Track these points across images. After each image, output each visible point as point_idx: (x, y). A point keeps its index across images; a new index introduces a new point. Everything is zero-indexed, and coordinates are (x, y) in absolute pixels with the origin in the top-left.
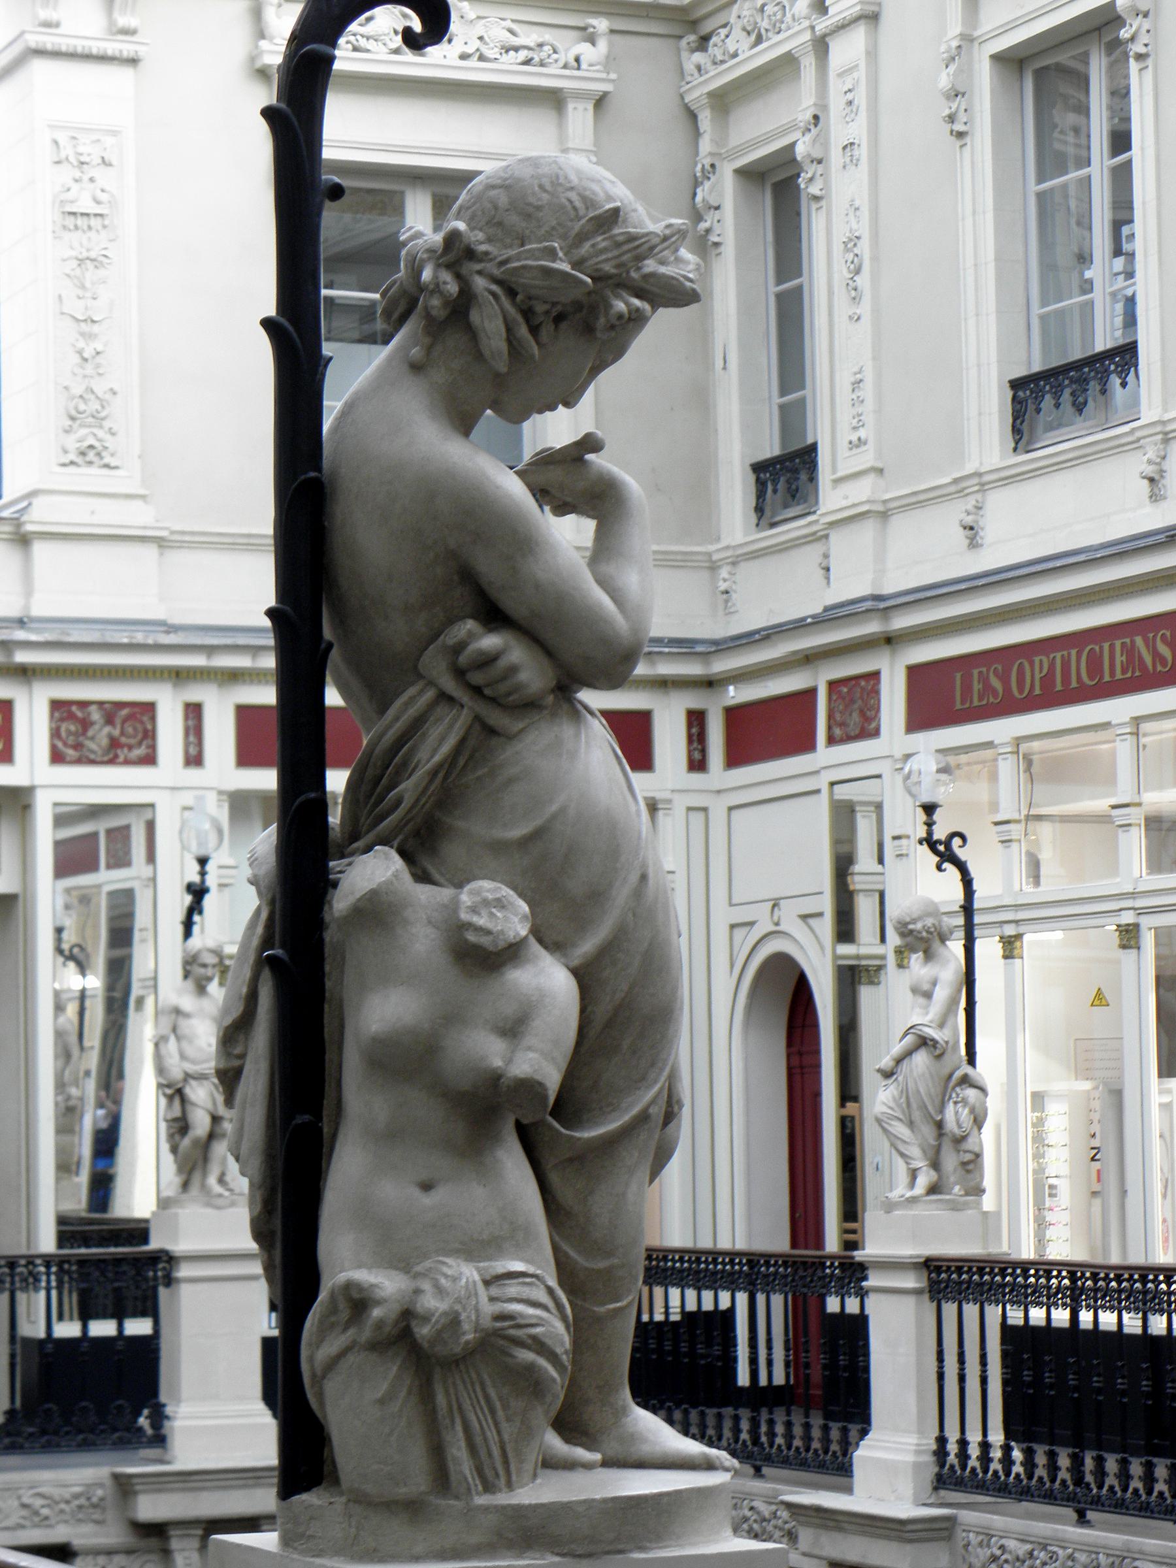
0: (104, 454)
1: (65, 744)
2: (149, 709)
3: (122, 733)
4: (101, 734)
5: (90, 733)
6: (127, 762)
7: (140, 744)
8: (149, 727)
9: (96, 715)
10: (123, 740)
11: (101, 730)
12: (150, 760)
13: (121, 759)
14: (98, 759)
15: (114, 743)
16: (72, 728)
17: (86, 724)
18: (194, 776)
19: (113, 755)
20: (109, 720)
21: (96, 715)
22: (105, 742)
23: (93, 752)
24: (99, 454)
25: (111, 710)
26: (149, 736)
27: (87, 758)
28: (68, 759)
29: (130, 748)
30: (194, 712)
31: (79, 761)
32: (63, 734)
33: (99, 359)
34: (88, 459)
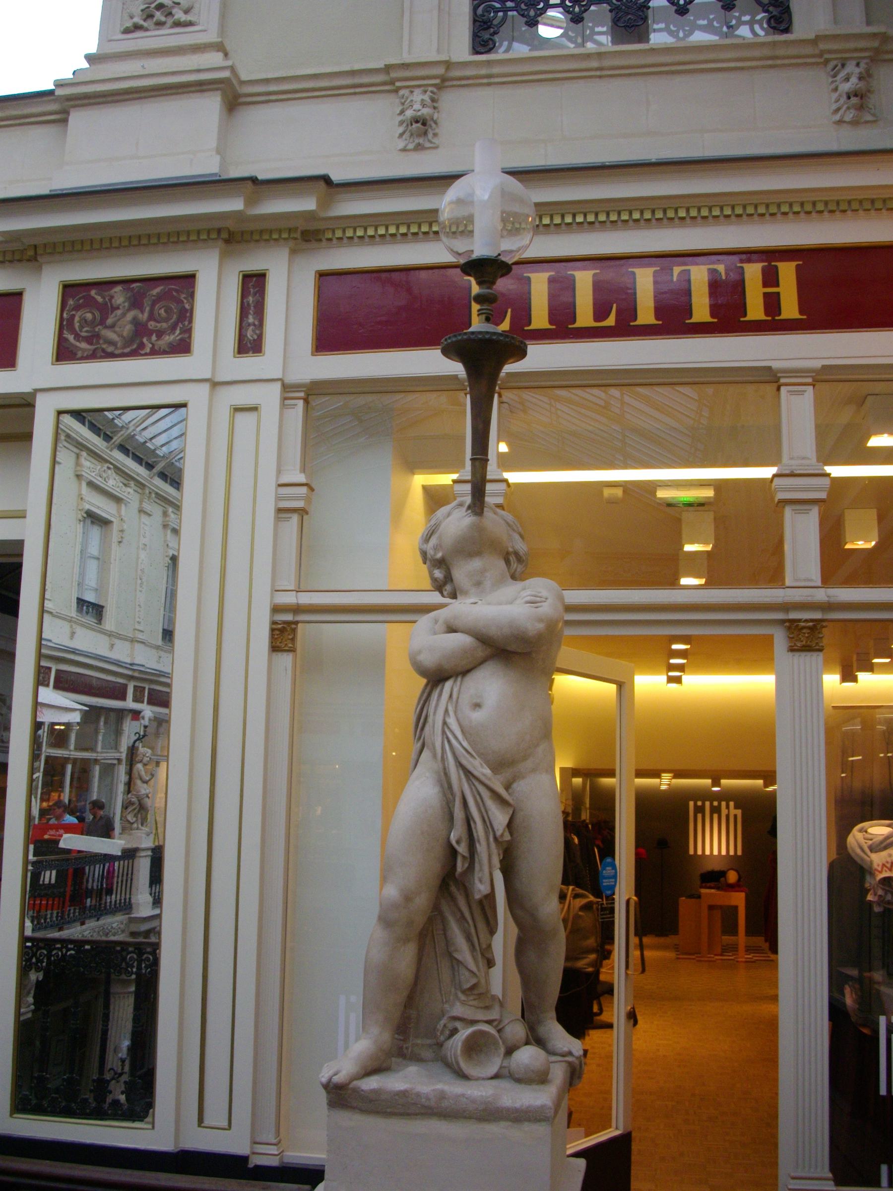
1: (78, 337)
3: (151, 317)
5: (109, 321)
6: (155, 352)
7: (173, 328)
8: (187, 306)
9: (119, 297)
10: (152, 325)
12: (183, 347)
13: (148, 350)
14: (117, 352)
15: (140, 330)
16: (89, 316)
17: (106, 309)
20: (136, 303)
22: (127, 329)
26: (186, 316)
27: (103, 350)
28: (79, 354)
29: (160, 334)
31: (93, 356)
32: (77, 325)
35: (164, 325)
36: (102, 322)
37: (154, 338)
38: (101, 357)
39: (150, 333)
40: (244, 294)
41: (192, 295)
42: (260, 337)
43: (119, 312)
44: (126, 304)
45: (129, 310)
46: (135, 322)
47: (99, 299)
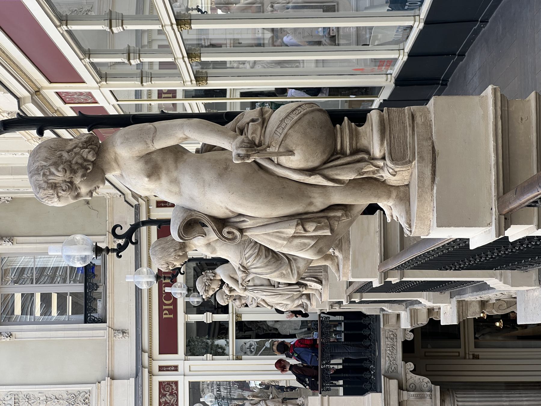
0: (86, 396)
2: (161, 383)
3: (168, 391)
4: (168, 398)
5: (169, 402)
6: (177, 390)
7: (171, 386)
9: (163, 400)
11: (167, 398)
12: (176, 383)
15: (171, 394)
18: (180, 368)
19: (175, 394)
20: (165, 395)
21: (163, 400)
22: (171, 397)
23: (174, 401)
24: (86, 398)
25: (162, 395)
26: (169, 383)
29: (173, 389)
30: (161, 368)
33: (57, 397)
34: (88, 401)
35: (171, 388)
36: (169, 403)
37: (173, 390)
38: (177, 403)
39: (172, 391)
40: (164, 371)
41: (164, 382)
42: (173, 366)
43: (167, 399)
44: (165, 398)
45: (166, 397)
46: (170, 395)
47: (163, 405)
